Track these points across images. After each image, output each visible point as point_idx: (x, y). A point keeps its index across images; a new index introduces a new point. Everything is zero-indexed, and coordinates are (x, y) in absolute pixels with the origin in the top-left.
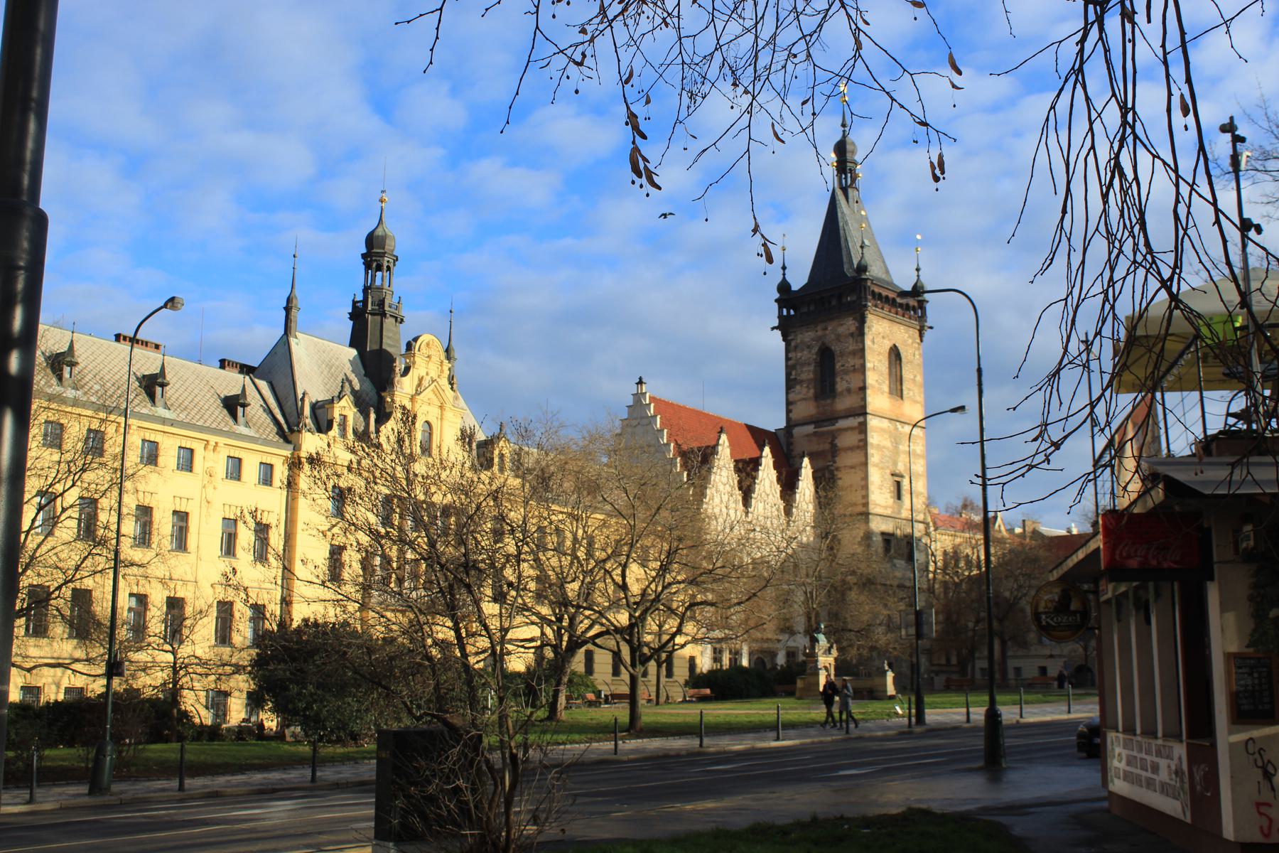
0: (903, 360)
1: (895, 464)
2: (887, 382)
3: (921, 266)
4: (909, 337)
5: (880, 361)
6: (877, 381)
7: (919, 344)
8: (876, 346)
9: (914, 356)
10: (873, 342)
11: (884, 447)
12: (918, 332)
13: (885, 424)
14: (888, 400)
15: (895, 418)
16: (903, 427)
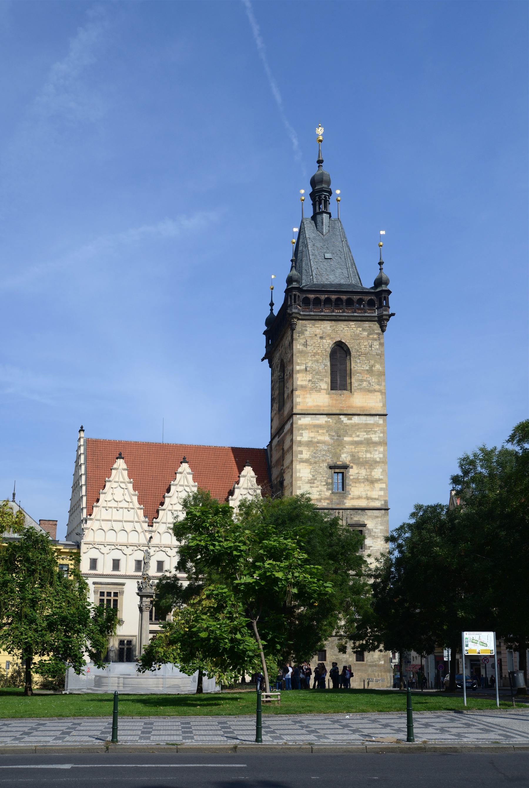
0: (353, 353)
1: (337, 456)
2: (328, 379)
3: (383, 260)
4: (364, 330)
5: (317, 361)
6: (309, 381)
7: (378, 334)
8: (309, 348)
9: (371, 347)
10: (306, 345)
11: (318, 442)
12: (377, 325)
13: (323, 420)
14: (327, 396)
15: (338, 412)
16: (350, 419)
